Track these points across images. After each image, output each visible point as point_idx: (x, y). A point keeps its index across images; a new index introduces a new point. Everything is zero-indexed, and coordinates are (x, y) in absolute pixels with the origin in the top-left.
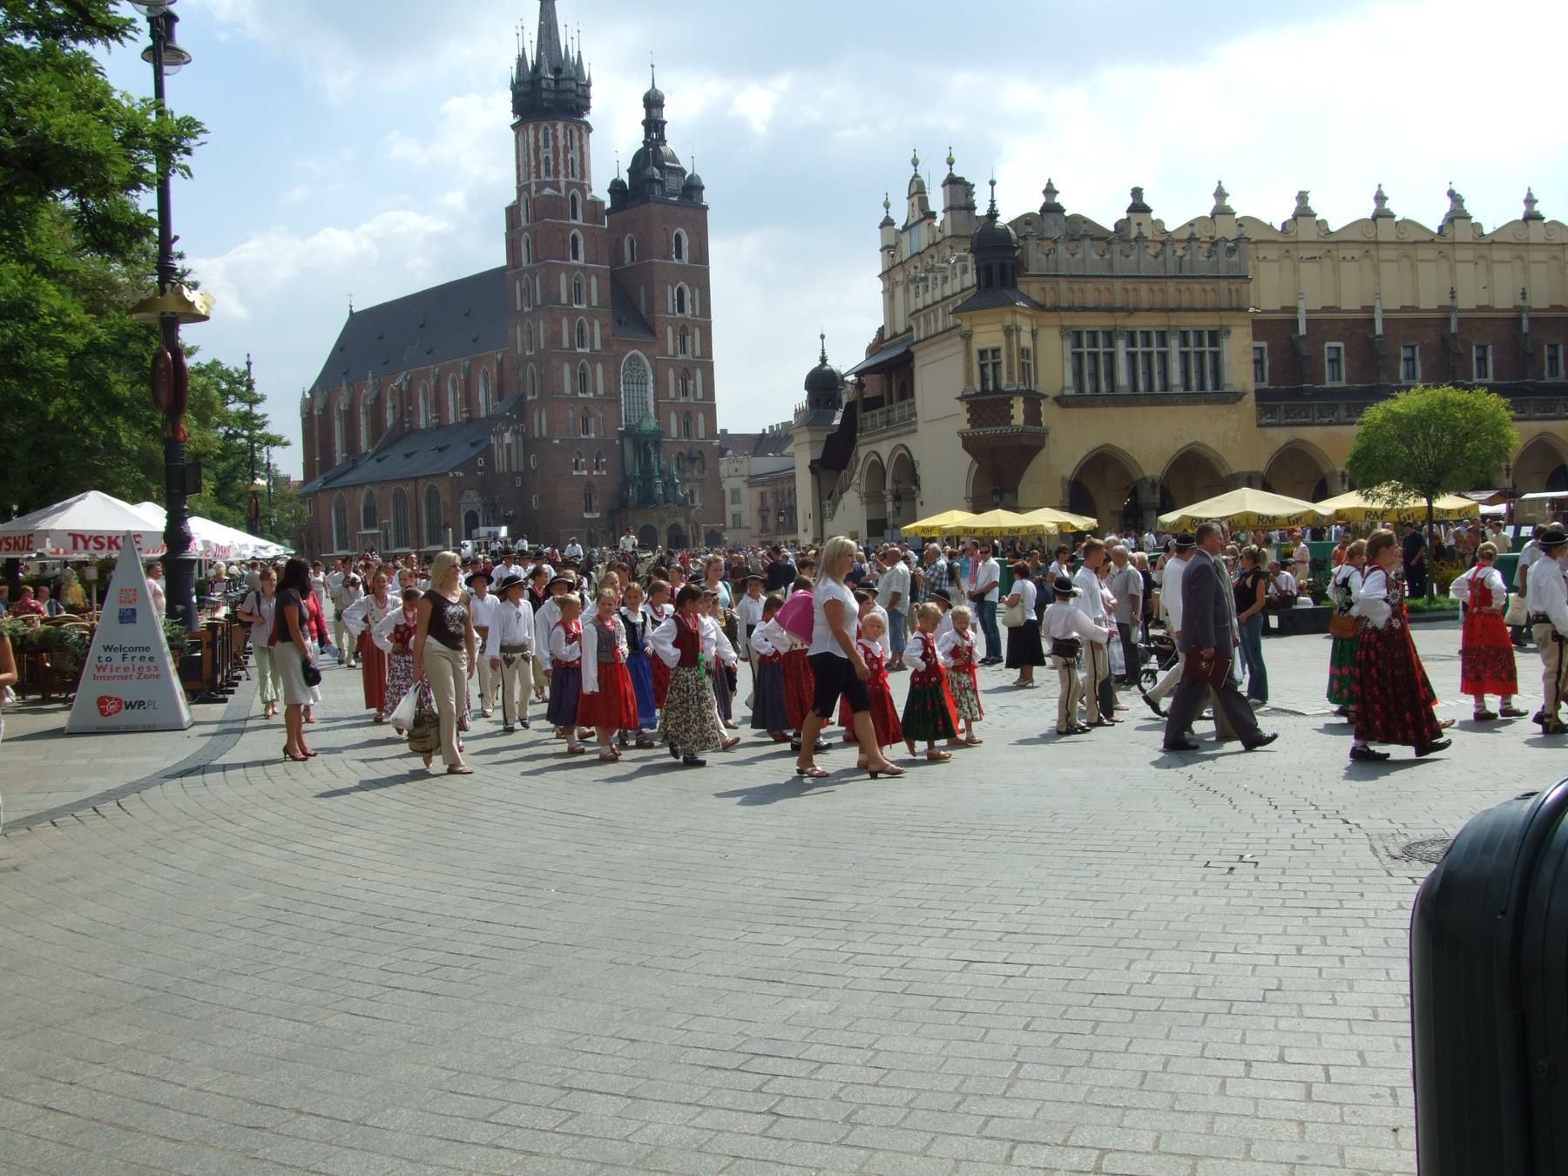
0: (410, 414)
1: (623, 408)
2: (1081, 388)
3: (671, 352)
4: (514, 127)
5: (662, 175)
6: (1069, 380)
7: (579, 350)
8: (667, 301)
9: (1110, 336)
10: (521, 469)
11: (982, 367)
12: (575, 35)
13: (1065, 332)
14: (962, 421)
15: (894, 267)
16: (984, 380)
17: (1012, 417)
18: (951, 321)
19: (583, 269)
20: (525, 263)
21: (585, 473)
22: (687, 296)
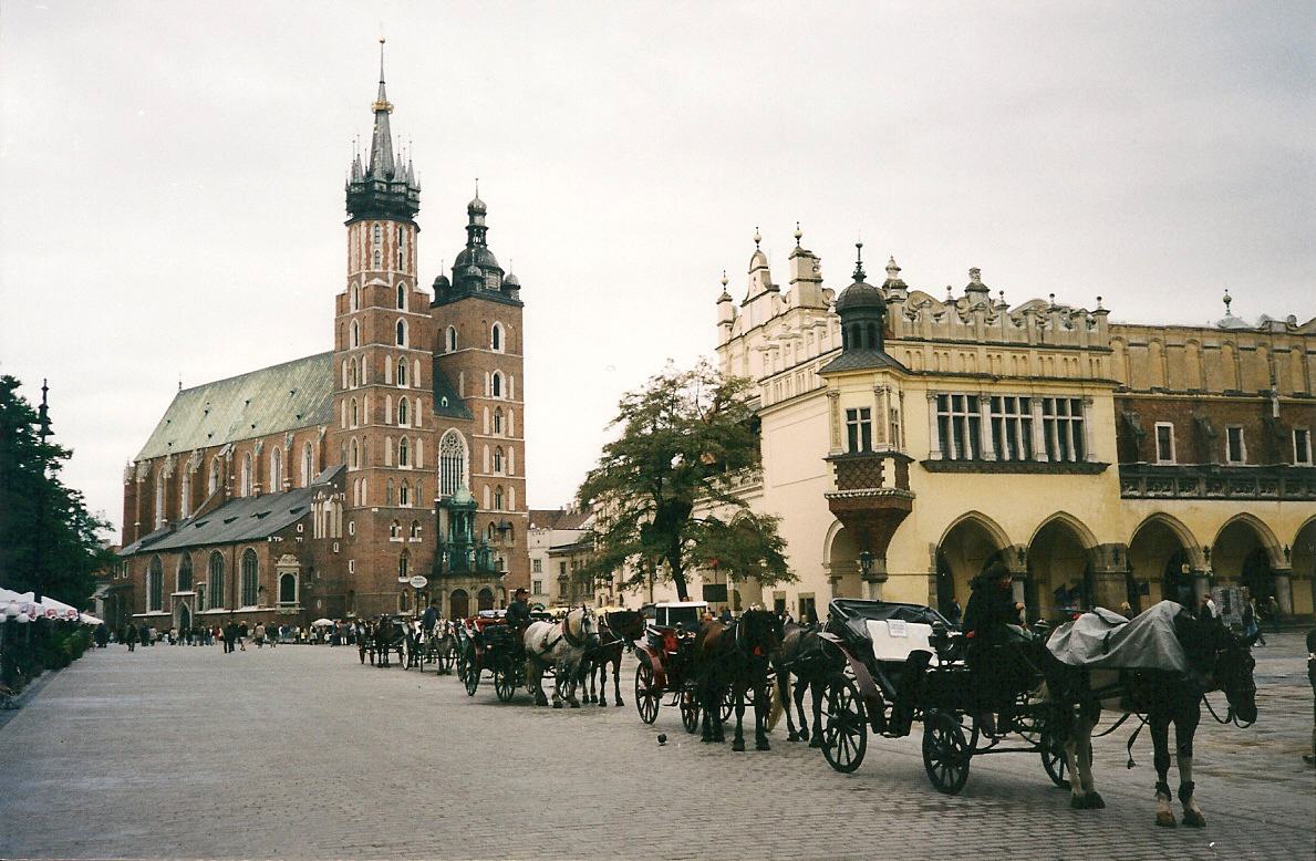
0: (233, 483)
1: (440, 481)
2: (945, 449)
3: (487, 431)
4: (347, 224)
5: (484, 273)
6: (936, 445)
7: (401, 426)
8: (484, 385)
9: (974, 402)
10: (340, 536)
11: (852, 429)
12: (407, 146)
13: (930, 395)
14: (828, 481)
15: (731, 340)
16: (853, 444)
17: (883, 479)
18: (818, 381)
19: (405, 352)
20: (352, 347)
21: (401, 540)
22: (503, 383)
